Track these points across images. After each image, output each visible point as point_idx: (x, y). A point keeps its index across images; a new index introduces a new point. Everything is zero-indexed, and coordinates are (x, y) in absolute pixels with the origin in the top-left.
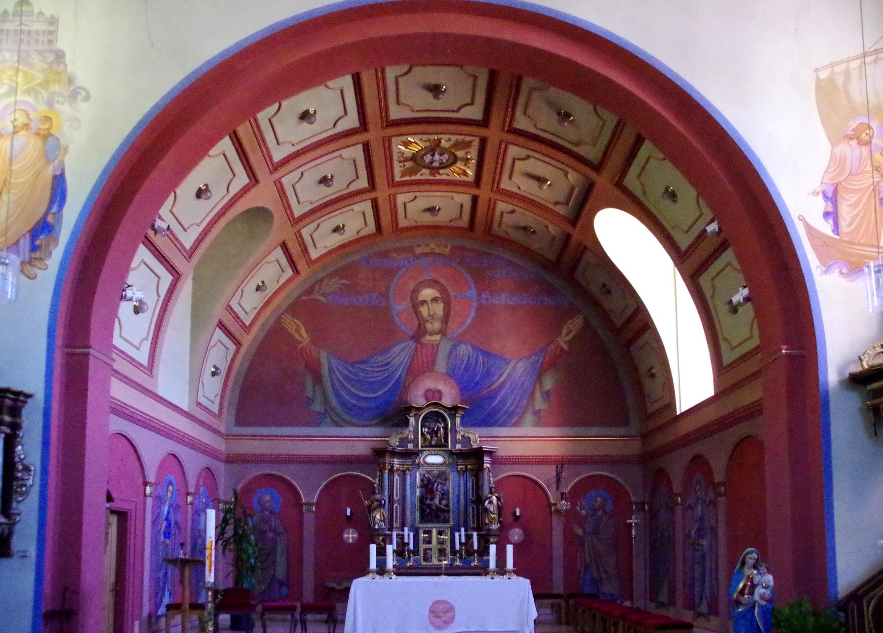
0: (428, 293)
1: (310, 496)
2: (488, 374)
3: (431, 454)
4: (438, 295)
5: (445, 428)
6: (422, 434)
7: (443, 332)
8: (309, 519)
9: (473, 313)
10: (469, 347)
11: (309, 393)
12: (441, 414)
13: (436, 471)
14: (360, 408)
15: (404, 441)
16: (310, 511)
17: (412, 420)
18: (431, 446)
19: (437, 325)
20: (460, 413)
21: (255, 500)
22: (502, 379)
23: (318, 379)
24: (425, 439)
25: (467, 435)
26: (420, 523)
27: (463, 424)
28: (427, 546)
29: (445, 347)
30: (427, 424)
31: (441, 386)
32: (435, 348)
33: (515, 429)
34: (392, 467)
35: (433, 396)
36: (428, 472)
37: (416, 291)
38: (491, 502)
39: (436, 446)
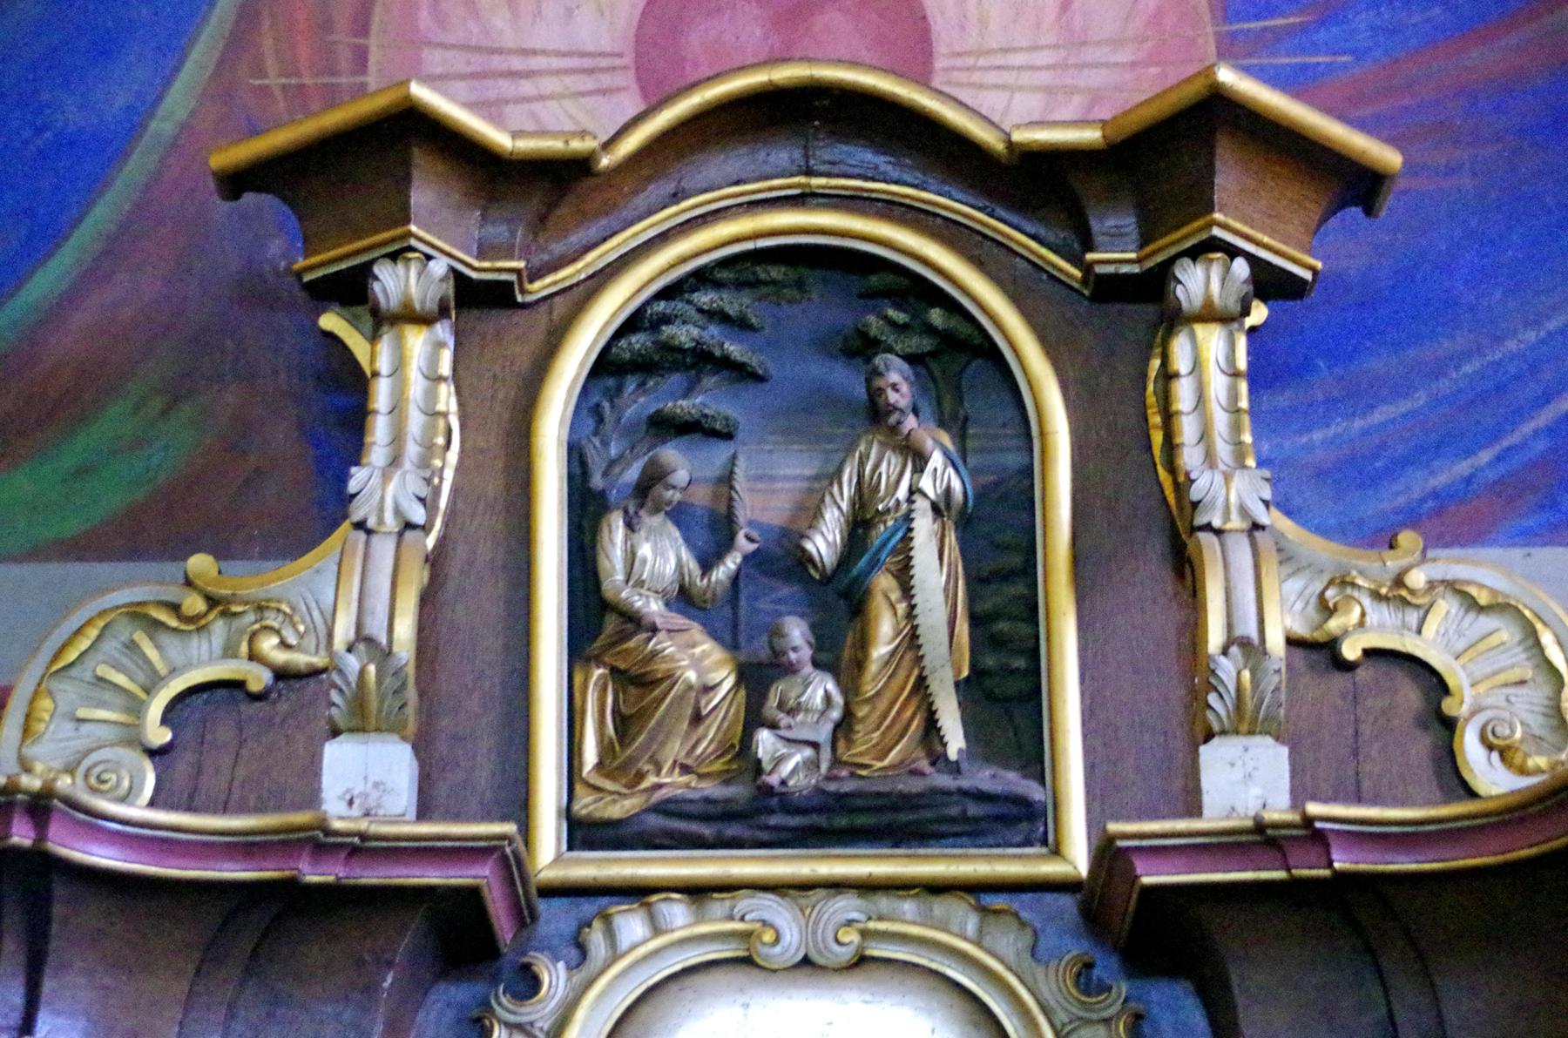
5: (996, 534)
6: (592, 611)
12: (919, 291)
15: (246, 725)
17: (413, 376)
18: (755, 814)
20: (1255, 220)
25: (1365, 628)
30: (683, 464)
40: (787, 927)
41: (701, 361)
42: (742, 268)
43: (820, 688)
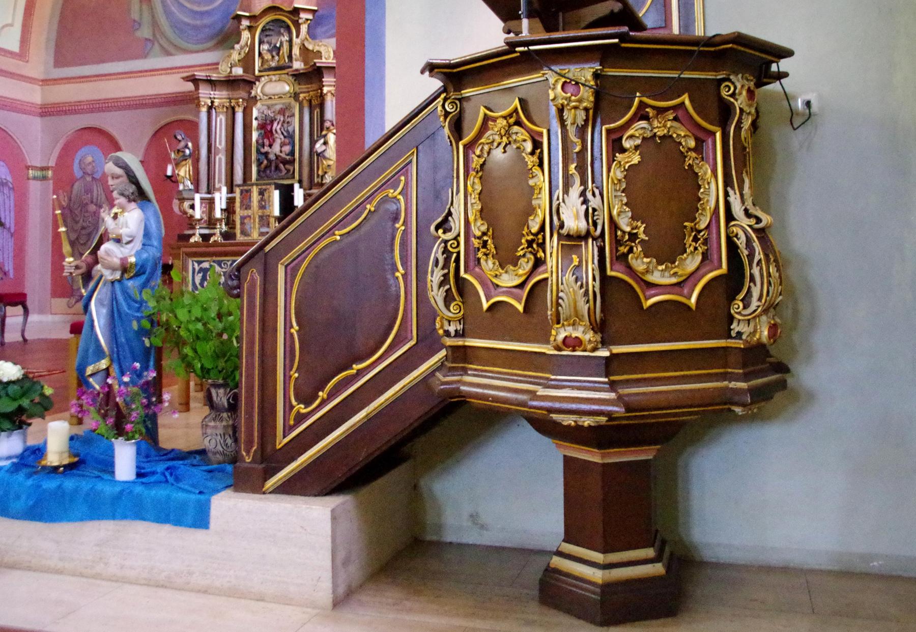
3: (271, 81)
11: (135, 15)
12: (284, 22)
14: (195, 28)
21: (77, 161)
28: (246, 213)
34: (212, 102)
40: (274, 78)
41: (270, 29)
42: (273, 21)
43: (277, 58)
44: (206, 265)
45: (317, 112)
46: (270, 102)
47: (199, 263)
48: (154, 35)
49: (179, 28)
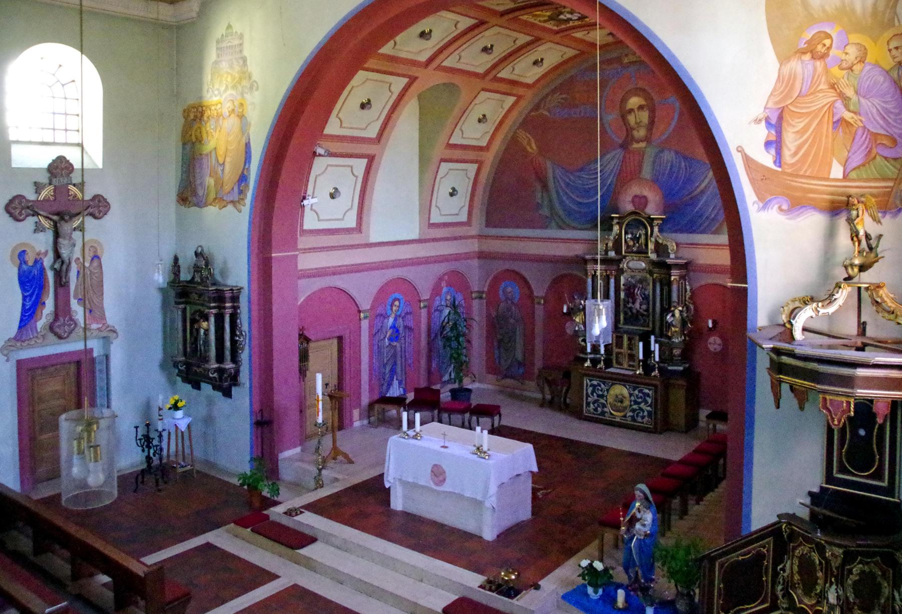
0: (634, 101)
1: (539, 291)
2: (689, 180)
4: (643, 102)
7: (647, 139)
8: (539, 312)
9: (676, 116)
10: (673, 154)
13: (639, 276)
16: (539, 303)
18: (632, 252)
19: (641, 133)
21: (501, 292)
22: (703, 185)
23: (545, 187)
24: (628, 246)
26: (624, 324)
27: (661, 231)
29: (650, 153)
31: (646, 192)
32: (641, 154)
33: (717, 236)
35: (640, 201)
36: (632, 277)
37: (624, 100)
38: (673, 316)
39: (638, 252)
44: (595, 383)
45: (666, 288)
46: (633, 274)
47: (591, 381)
48: (552, 214)
49: (569, 213)
